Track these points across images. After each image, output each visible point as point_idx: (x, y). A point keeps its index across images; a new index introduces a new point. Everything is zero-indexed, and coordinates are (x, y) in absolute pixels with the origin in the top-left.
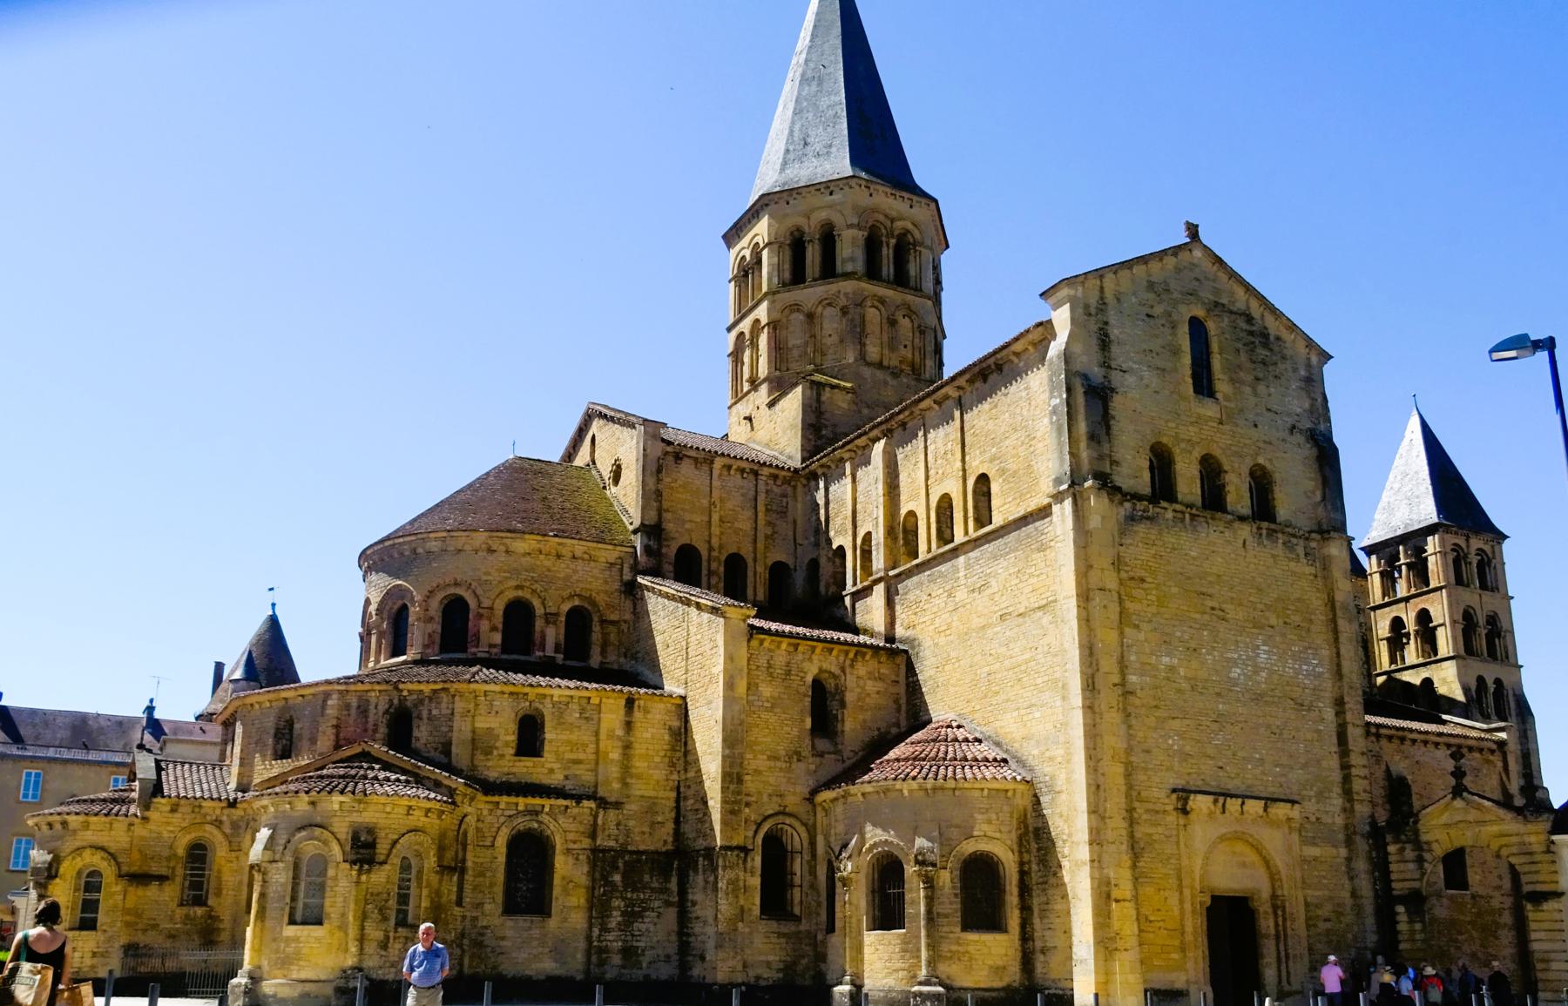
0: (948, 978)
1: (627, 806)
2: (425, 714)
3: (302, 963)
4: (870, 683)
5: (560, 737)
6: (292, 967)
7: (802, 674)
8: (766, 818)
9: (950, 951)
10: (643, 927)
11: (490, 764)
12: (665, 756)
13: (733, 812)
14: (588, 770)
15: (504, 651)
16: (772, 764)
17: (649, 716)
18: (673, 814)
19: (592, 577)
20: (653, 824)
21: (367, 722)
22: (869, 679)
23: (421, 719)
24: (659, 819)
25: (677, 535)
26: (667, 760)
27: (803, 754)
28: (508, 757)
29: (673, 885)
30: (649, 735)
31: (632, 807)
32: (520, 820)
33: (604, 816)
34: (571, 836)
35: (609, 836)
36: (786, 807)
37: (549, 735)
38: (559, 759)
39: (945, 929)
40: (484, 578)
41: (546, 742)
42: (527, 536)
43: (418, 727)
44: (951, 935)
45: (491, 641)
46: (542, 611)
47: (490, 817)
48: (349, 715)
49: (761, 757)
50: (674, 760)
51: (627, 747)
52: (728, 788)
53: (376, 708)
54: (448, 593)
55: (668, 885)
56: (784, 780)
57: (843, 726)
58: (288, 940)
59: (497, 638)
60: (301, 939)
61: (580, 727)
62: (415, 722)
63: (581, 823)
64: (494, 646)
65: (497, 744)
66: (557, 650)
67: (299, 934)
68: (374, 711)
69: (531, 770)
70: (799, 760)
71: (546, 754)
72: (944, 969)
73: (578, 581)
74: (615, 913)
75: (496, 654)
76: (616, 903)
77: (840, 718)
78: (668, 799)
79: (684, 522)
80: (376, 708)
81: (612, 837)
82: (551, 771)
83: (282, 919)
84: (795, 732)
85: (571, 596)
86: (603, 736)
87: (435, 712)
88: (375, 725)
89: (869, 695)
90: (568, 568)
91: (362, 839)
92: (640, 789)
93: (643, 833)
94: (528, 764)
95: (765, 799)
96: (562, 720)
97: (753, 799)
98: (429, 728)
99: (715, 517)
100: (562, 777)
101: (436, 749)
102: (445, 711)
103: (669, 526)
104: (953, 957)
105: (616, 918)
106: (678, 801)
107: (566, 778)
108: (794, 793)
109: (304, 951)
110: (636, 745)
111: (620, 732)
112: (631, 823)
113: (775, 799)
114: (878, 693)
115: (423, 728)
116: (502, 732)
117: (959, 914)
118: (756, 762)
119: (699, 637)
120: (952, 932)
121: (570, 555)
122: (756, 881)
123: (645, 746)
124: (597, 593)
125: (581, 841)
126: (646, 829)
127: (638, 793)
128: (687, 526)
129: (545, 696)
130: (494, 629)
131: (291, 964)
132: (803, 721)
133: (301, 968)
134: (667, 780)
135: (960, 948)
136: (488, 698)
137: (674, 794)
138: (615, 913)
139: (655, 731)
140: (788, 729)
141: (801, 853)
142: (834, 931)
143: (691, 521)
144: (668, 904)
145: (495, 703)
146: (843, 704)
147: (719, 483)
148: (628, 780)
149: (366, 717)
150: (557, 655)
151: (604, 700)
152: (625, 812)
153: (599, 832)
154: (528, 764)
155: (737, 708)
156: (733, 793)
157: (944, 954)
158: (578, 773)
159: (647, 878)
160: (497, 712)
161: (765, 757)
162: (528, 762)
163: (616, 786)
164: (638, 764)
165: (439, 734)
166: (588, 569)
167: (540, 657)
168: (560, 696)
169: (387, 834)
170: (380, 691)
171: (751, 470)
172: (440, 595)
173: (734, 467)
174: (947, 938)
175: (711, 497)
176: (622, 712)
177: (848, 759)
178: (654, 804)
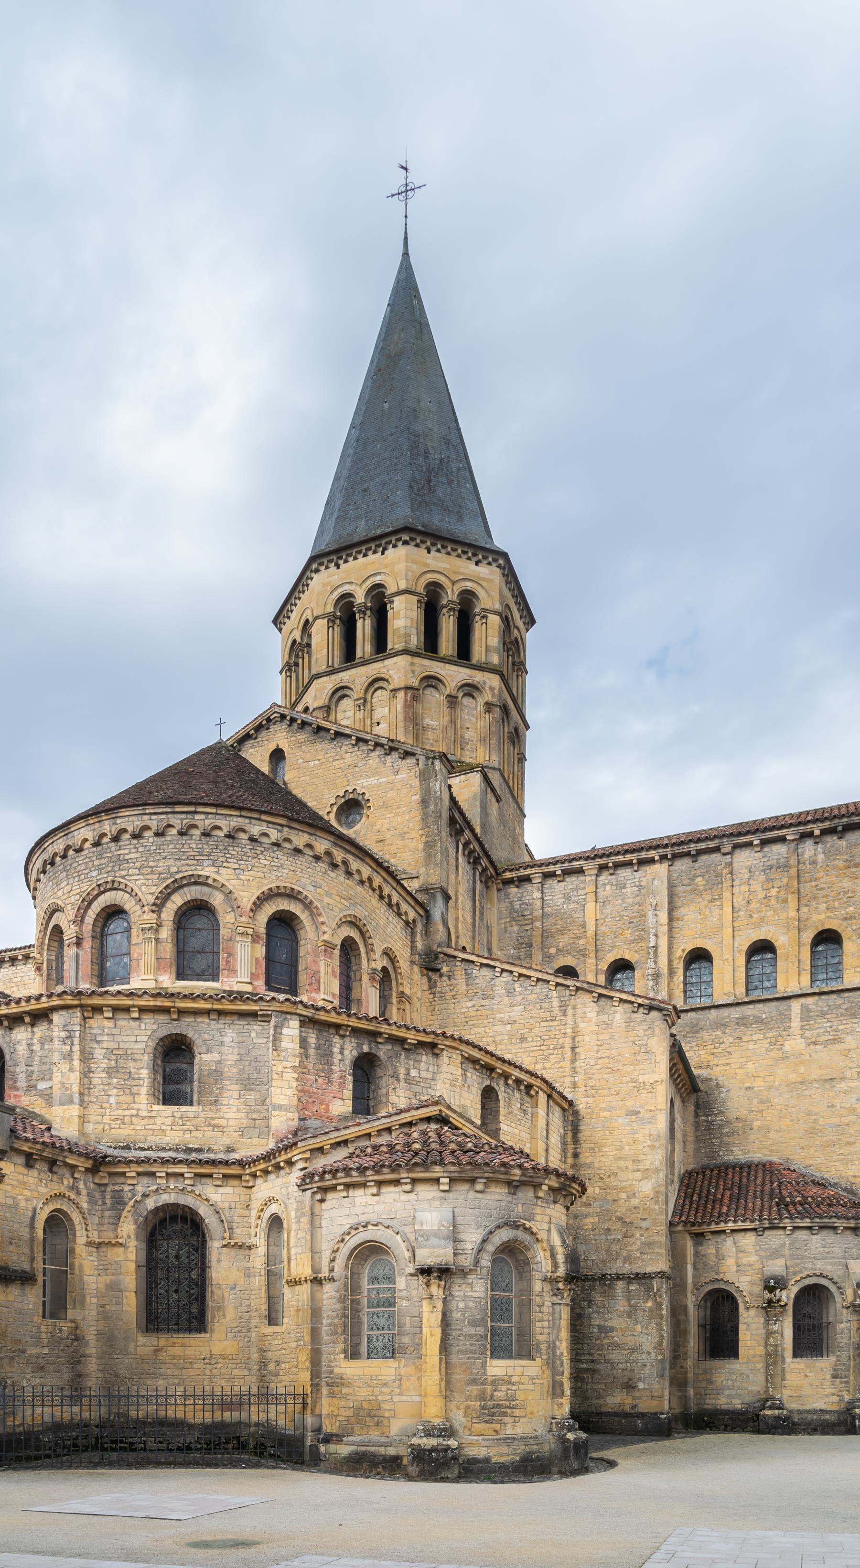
2: (402, 1071)
3: (517, 1412)
5: (510, 1129)
6: (506, 1419)
21: (331, 1071)
43: (394, 1089)
53: (341, 1053)
54: (281, 908)
58: (496, 1382)
60: (514, 1379)
67: (510, 1371)
80: (341, 1053)
83: (483, 1353)
87: (413, 1073)
88: (341, 1077)
102: (424, 1074)
109: (520, 1395)
115: (400, 1092)
119: (601, 1037)
131: (505, 1414)
133: (516, 1419)
149: (330, 1063)
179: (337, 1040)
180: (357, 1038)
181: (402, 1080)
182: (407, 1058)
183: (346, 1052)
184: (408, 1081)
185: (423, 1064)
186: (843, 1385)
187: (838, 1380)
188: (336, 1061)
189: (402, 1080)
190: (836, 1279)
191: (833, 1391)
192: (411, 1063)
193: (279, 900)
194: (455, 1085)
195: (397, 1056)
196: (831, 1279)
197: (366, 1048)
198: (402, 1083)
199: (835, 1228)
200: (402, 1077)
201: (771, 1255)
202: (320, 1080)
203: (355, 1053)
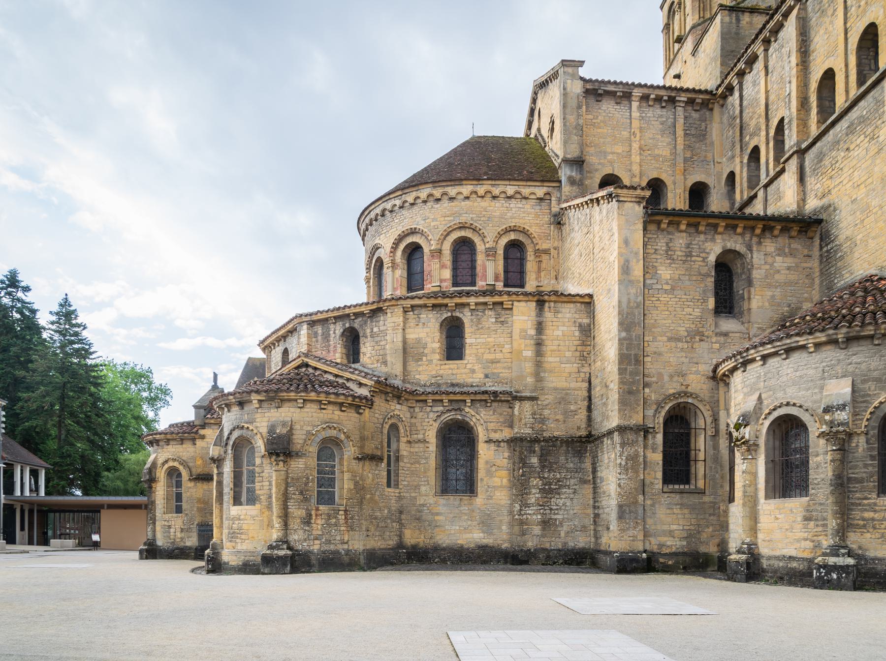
0: (860, 548)
1: (542, 398)
4: (779, 259)
5: (479, 341)
7: (703, 255)
8: (669, 397)
9: (863, 519)
10: (561, 502)
11: (420, 369)
12: (576, 350)
13: (630, 392)
14: (504, 368)
15: (455, 284)
16: (673, 344)
17: (560, 315)
18: (586, 403)
19: (524, 212)
20: (566, 413)
21: (329, 345)
22: (779, 255)
23: (366, 337)
24: (572, 408)
25: (600, 167)
26: (578, 354)
27: (706, 334)
28: (435, 361)
29: (588, 465)
30: (560, 333)
31: (547, 399)
32: (446, 416)
33: (520, 407)
34: (491, 426)
35: (525, 424)
36: (687, 386)
37: (469, 339)
38: (479, 359)
39: (858, 495)
40: (432, 224)
41: (467, 346)
42: (464, 182)
44: (865, 502)
45: (442, 278)
46: (483, 247)
47: (421, 414)
48: (317, 341)
49: (660, 338)
50: (585, 353)
51: (539, 344)
52: (626, 369)
53: (334, 333)
55: (583, 466)
56: (686, 360)
57: (749, 303)
59: (447, 274)
61: (496, 331)
62: (362, 340)
63: (501, 414)
64: (445, 280)
65: (426, 351)
66: (497, 279)
68: (333, 335)
69: (454, 372)
70: (701, 340)
71: (467, 357)
72: (854, 539)
73: (512, 218)
74: (534, 491)
75: (446, 288)
76: (535, 482)
77: (746, 297)
78: (580, 389)
79: (605, 153)
80: (334, 333)
81: (528, 425)
82: (473, 371)
84: (697, 312)
85: (507, 231)
86: (516, 336)
87: (375, 330)
89: (778, 271)
90: (502, 207)
91: (278, 431)
92: (554, 381)
93: (557, 420)
94: (452, 366)
95: (666, 378)
96: (480, 326)
97: (654, 379)
98: (373, 344)
99: (635, 146)
100: (482, 376)
101: (378, 361)
103: (592, 159)
104: (868, 525)
105: (534, 496)
106: (589, 390)
107: (486, 376)
108: (697, 372)
110: (547, 343)
111: (532, 332)
112: (546, 412)
113: (676, 379)
114: (789, 268)
116: (429, 340)
117: (876, 477)
118: (657, 344)
120: (866, 498)
121: (503, 195)
122: (657, 457)
123: (556, 343)
124: (530, 227)
125: (502, 430)
126: (560, 417)
127: (551, 385)
128: (610, 157)
129: (463, 305)
130: (443, 266)
132: (705, 301)
134: (579, 372)
135: (876, 516)
136: (416, 312)
137: (587, 384)
138: (534, 491)
139: (565, 328)
140: (689, 310)
141: (705, 429)
142: (733, 501)
143: (613, 153)
144: (583, 482)
145: (422, 316)
146: (750, 282)
147: (638, 114)
148: (542, 375)
149: (328, 341)
150: (497, 284)
151: (515, 303)
152: (539, 402)
153: (516, 421)
154: (452, 366)
155: (633, 291)
156: (631, 373)
157: (856, 522)
158: (495, 371)
159: (562, 459)
160: (424, 324)
161: (665, 339)
162: (453, 364)
163: (530, 380)
164: (550, 359)
165: (379, 348)
166: (521, 206)
167: (483, 286)
168: (476, 304)
169: (302, 427)
170: (335, 318)
171: (669, 97)
172: (402, 246)
173: (652, 96)
174: (860, 504)
175: (631, 128)
176: (533, 314)
177: (755, 336)
178: (567, 394)
179: (332, 326)
180: (343, 321)
181: (369, 337)
182: (372, 322)
183: (337, 332)
184: (372, 336)
185: (381, 322)
186: (820, 529)
187: (812, 523)
188: (332, 339)
189: (369, 337)
190: (806, 405)
191: (806, 535)
192: (374, 324)
193: (407, 238)
194: (397, 329)
195: (366, 323)
196: (801, 407)
197: (347, 325)
198: (369, 338)
199: (804, 347)
200: (369, 334)
201: (751, 389)
202: (324, 352)
203: (342, 330)
